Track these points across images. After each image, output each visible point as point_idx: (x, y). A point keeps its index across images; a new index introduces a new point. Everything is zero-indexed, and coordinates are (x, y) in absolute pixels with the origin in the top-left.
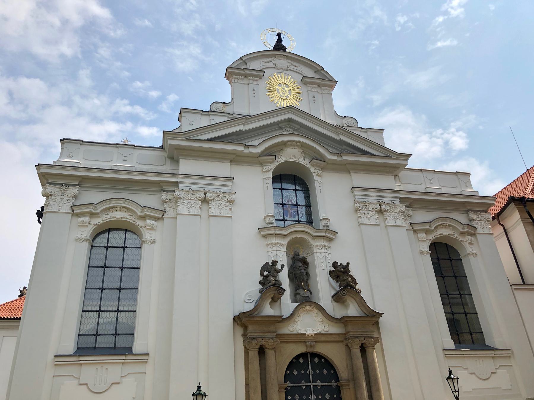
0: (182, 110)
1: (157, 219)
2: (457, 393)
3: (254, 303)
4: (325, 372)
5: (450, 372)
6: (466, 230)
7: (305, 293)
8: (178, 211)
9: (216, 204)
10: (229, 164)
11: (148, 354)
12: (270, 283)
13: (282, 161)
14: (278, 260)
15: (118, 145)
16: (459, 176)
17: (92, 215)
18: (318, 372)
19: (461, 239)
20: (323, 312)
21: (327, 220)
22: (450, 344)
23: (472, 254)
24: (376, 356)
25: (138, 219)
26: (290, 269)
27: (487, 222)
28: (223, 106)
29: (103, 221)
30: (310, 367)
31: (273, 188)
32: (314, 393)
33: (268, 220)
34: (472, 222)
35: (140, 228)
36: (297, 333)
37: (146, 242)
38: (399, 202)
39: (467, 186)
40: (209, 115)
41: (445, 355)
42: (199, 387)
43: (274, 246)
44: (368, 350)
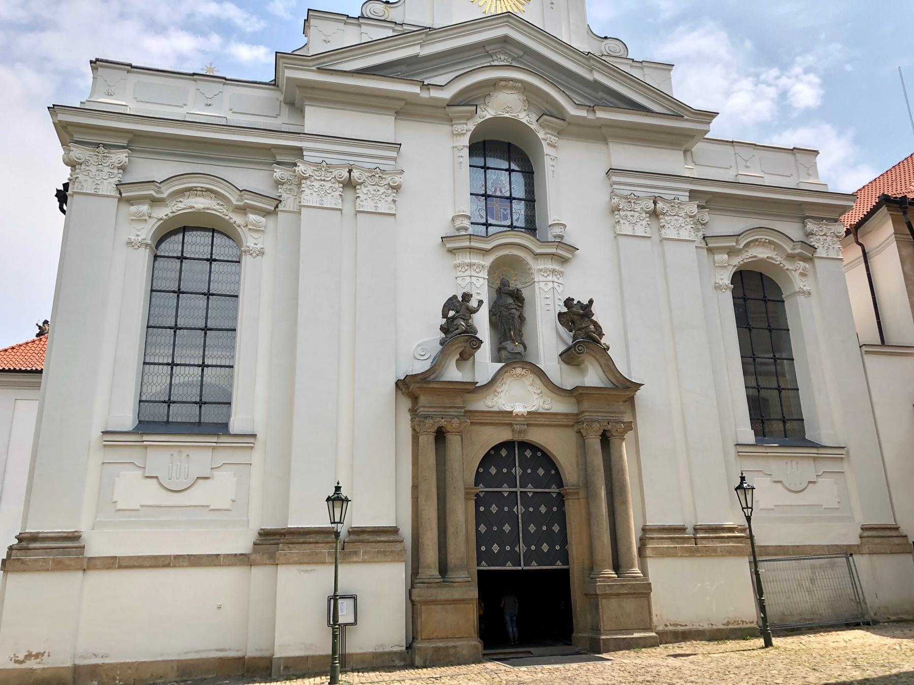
0: (310, 13)
1: (266, 213)
2: (750, 510)
3: (431, 360)
4: (541, 472)
5: (743, 478)
6: (798, 251)
7: (516, 347)
8: (302, 200)
9: (369, 190)
10: (394, 117)
11: (254, 436)
12: (458, 329)
13: (488, 116)
14: (473, 292)
15: (195, 77)
16: (798, 156)
17: (154, 202)
18: (529, 471)
19: (788, 265)
20: (543, 379)
21: (562, 227)
22: (749, 436)
23: (803, 292)
24: (625, 450)
25: (233, 211)
26: (493, 308)
27: (835, 239)
28: (386, 8)
29: (173, 212)
30: (517, 464)
31: (470, 166)
32: (521, 504)
33: (458, 223)
34: (810, 238)
35: (238, 228)
36: (498, 410)
37: (248, 252)
38: (687, 199)
39: (809, 174)
40: (359, 25)
41: (738, 452)
42: (338, 488)
43: (466, 268)
44: (614, 441)
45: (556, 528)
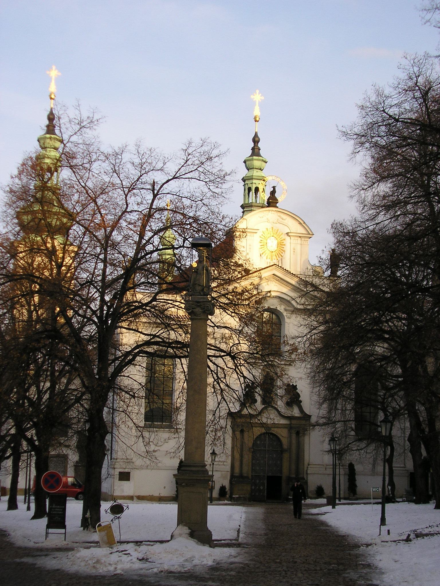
44: (301, 435)
45: (279, 462)
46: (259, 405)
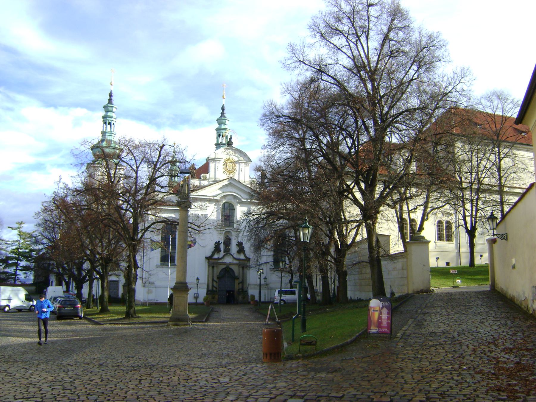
46: (222, 254)
